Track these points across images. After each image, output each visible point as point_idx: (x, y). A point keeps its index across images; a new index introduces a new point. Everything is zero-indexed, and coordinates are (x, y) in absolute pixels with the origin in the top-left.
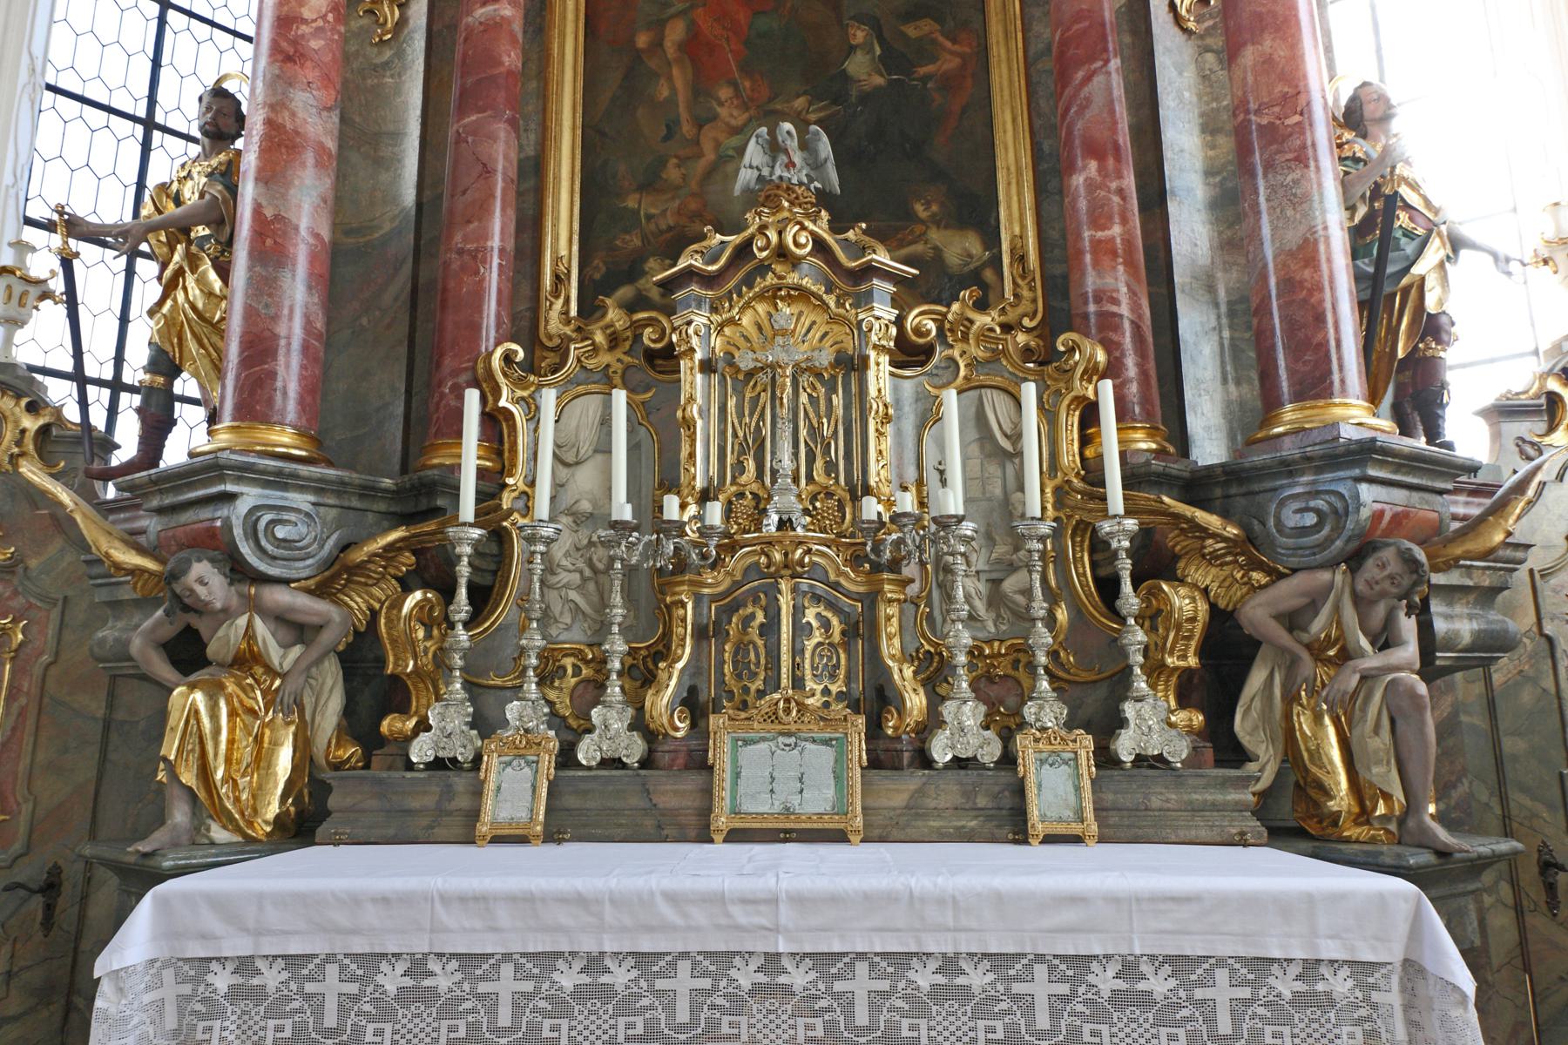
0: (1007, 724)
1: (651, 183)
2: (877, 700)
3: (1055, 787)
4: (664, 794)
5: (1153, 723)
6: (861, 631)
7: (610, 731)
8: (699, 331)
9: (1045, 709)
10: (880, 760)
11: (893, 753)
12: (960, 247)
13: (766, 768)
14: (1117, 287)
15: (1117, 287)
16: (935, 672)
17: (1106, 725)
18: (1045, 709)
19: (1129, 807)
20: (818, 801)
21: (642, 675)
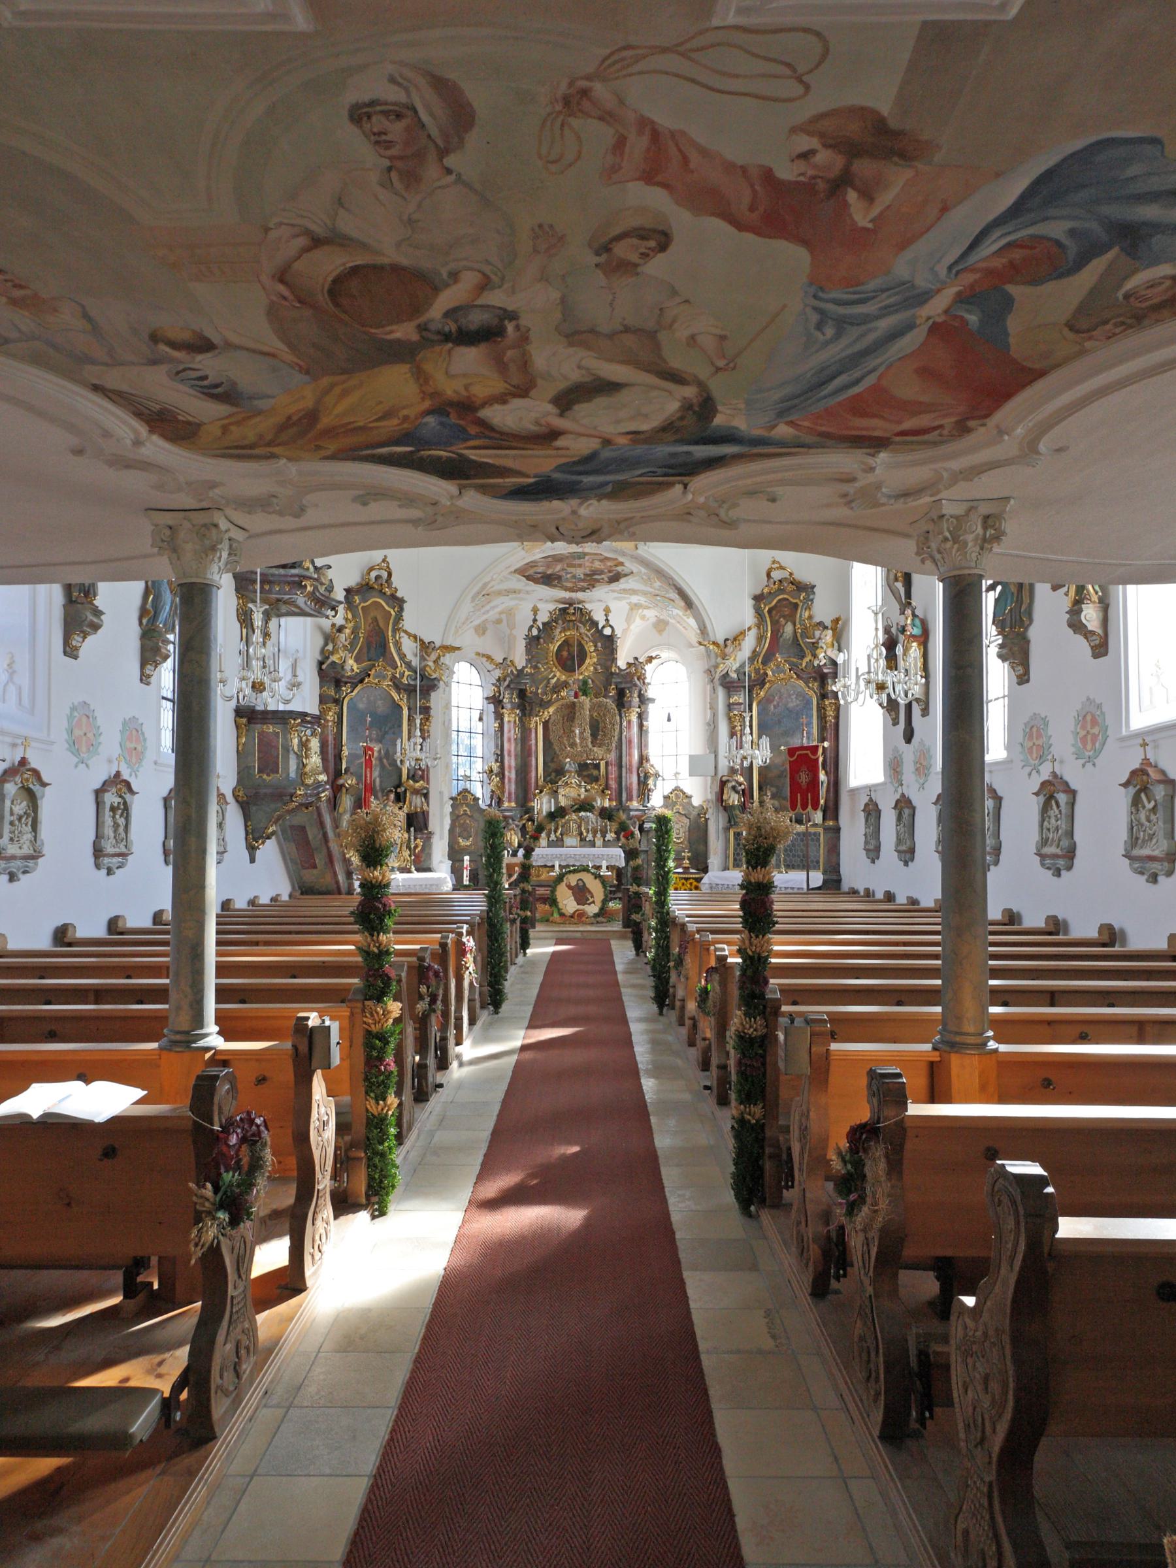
0: (594, 836)
1: (552, 761)
2: (581, 834)
3: (599, 842)
4: (559, 843)
5: (610, 836)
6: (580, 826)
7: (553, 837)
8: (561, 791)
9: (599, 835)
10: (581, 840)
11: (583, 839)
12: (595, 772)
13: (570, 841)
14: (613, 784)
15: (613, 784)
16: (588, 832)
17: (604, 836)
18: (599, 835)
19: (606, 844)
20: (574, 844)
21: (555, 832)
